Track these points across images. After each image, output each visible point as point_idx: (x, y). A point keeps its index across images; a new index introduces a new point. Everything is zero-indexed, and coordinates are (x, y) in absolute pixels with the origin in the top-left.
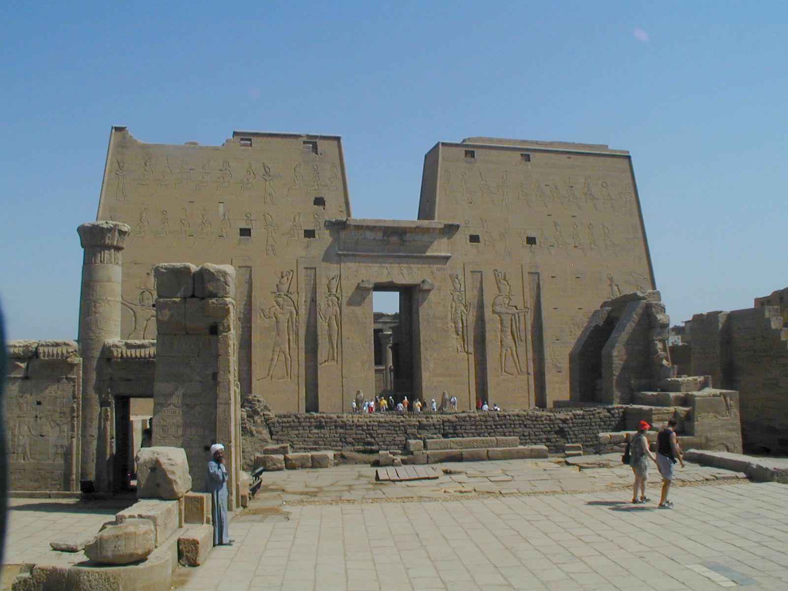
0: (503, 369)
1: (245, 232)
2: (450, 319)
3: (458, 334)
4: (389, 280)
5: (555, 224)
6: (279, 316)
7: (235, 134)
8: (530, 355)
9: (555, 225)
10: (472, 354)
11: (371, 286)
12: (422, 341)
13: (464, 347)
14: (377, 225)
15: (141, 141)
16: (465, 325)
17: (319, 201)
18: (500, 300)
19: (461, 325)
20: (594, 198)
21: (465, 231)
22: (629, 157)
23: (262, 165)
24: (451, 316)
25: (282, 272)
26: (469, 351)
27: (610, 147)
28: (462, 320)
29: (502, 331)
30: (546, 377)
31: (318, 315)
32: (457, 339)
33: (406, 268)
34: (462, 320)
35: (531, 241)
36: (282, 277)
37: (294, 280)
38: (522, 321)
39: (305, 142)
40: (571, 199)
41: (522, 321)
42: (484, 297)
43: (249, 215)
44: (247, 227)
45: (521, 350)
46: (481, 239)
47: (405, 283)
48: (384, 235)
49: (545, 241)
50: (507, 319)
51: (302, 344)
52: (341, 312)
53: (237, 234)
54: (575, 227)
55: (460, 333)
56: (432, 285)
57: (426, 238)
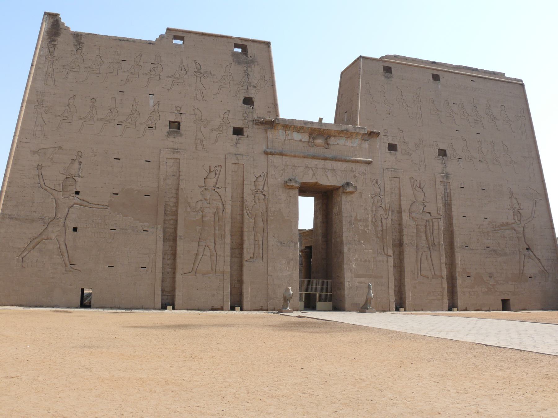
1: (175, 126)
2: (370, 221)
3: (378, 237)
4: (314, 180)
7: (168, 29)
8: (443, 259)
11: (297, 185)
12: (345, 242)
15: (74, 28)
16: (384, 228)
17: (248, 101)
19: (380, 228)
22: (523, 85)
23: (194, 62)
25: (210, 167)
27: (506, 76)
28: (382, 223)
30: (458, 281)
31: (245, 212)
34: (382, 223)
35: (443, 153)
37: (222, 176)
39: (236, 46)
40: (475, 118)
41: (435, 227)
42: (402, 203)
43: (179, 109)
44: (176, 120)
47: (328, 183)
48: (310, 137)
51: (228, 240)
52: (267, 208)
53: (166, 126)
55: (380, 235)
56: (356, 188)
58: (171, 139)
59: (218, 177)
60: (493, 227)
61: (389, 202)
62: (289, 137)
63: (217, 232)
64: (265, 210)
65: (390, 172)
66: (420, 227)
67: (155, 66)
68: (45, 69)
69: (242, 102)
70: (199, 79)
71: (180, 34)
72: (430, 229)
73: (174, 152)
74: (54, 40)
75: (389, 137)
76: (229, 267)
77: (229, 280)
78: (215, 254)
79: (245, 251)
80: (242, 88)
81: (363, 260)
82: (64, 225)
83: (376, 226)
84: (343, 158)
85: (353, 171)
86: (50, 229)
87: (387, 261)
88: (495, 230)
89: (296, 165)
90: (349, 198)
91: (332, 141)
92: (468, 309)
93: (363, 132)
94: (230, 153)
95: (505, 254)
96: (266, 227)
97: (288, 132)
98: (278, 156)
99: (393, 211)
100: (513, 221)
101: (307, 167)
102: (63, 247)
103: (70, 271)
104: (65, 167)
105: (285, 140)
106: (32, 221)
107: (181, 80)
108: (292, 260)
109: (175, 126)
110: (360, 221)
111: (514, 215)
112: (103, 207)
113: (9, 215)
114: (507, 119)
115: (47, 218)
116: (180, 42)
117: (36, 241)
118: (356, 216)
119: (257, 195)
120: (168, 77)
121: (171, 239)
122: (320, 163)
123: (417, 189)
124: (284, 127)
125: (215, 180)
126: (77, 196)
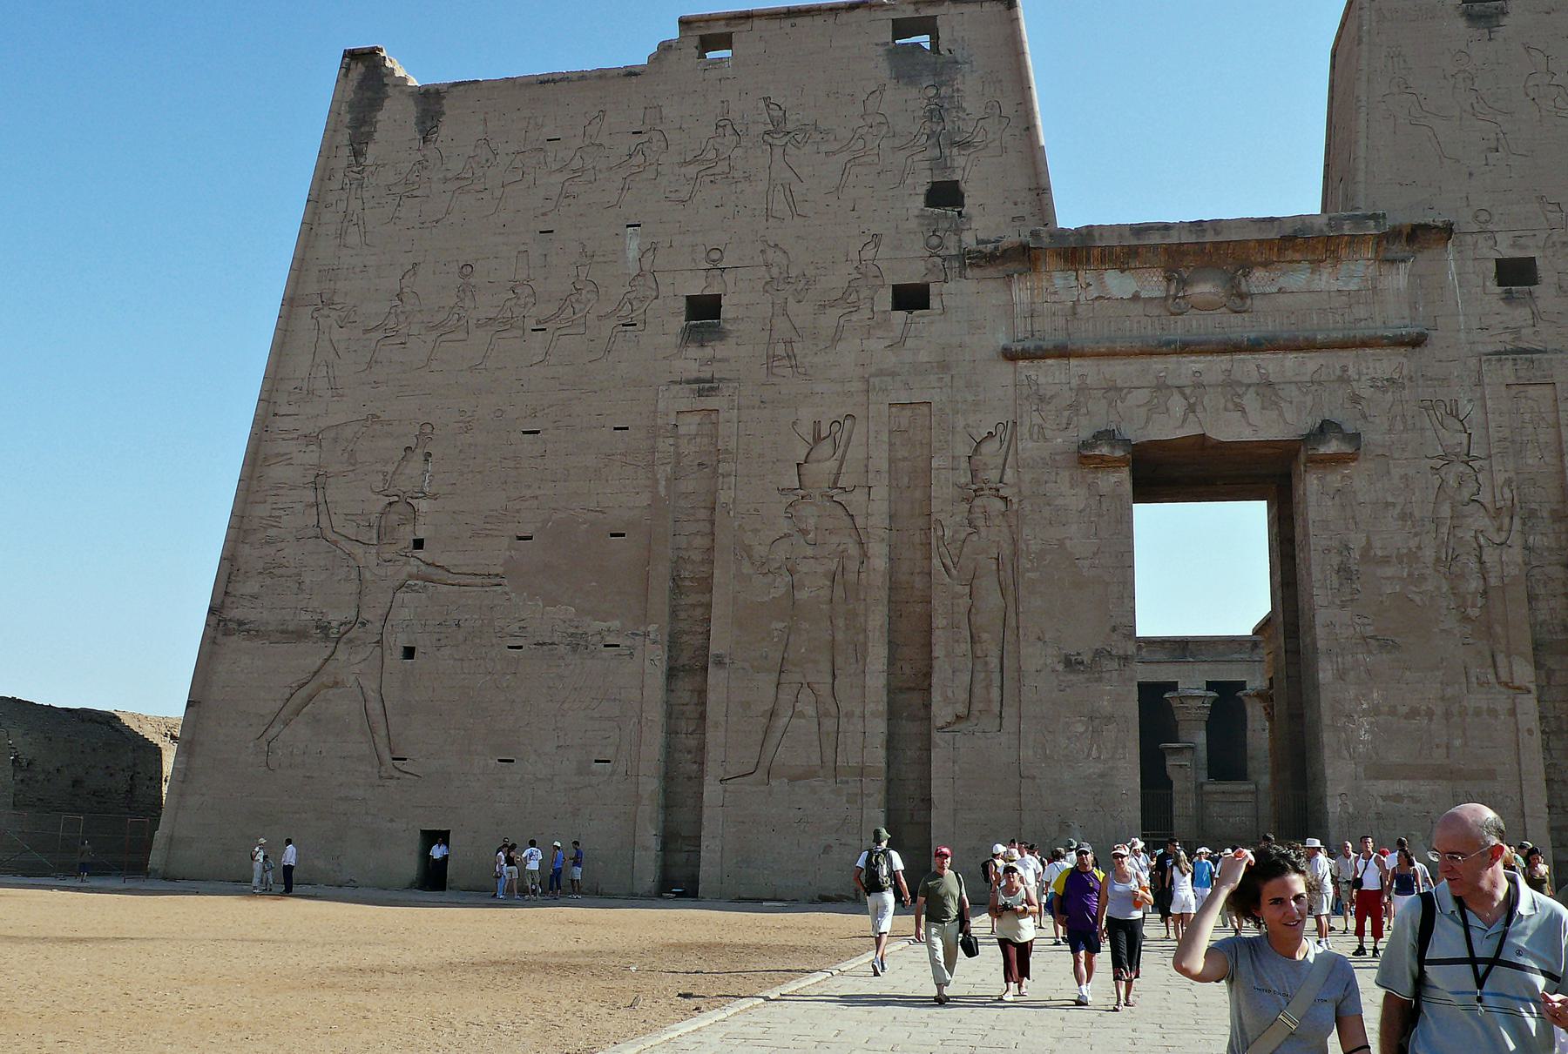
1: (704, 310)
3: (1466, 619)
4: (1191, 430)
6: (803, 568)
7: (685, 23)
11: (1119, 453)
12: (1321, 644)
13: (1495, 666)
14: (1136, 243)
16: (1493, 582)
17: (945, 195)
19: (1474, 584)
23: (762, 104)
25: (817, 423)
28: (1481, 562)
31: (936, 562)
33: (1252, 390)
34: (1481, 562)
36: (818, 439)
37: (855, 453)
43: (715, 255)
47: (1247, 435)
48: (1169, 280)
52: (1015, 542)
55: (1474, 612)
56: (1355, 438)
57: (1325, 280)
58: (693, 351)
59: (845, 452)
61: (1508, 482)
62: (1093, 292)
63: (840, 636)
64: (1007, 550)
67: (644, 138)
68: (342, 206)
69: (922, 198)
70: (778, 152)
71: (719, 28)
73: (700, 393)
74: (363, 122)
75: (1499, 237)
76: (882, 753)
77: (880, 797)
78: (833, 710)
79: (936, 697)
80: (920, 157)
81: (1404, 710)
82: (379, 643)
84: (1301, 335)
86: (341, 655)
87: (1513, 712)
89: (1119, 383)
90: (1334, 479)
91: (1259, 280)
93: (1371, 229)
94: (881, 373)
96: (1011, 609)
97: (1087, 276)
98: (1049, 361)
101: (1161, 387)
102: (375, 706)
103: (392, 778)
104: (385, 474)
105: (1075, 303)
106: (300, 635)
107: (722, 167)
108: (1110, 719)
109: (704, 310)
110: (1386, 561)
112: (486, 581)
113: (241, 623)
115: (334, 624)
116: (727, 53)
117: (304, 692)
118: (1369, 545)
119: (978, 502)
120: (686, 163)
121: (688, 666)
122: (1213, 367)
124: (1066, 260)
125: (832, 465)
126: (420, 554)
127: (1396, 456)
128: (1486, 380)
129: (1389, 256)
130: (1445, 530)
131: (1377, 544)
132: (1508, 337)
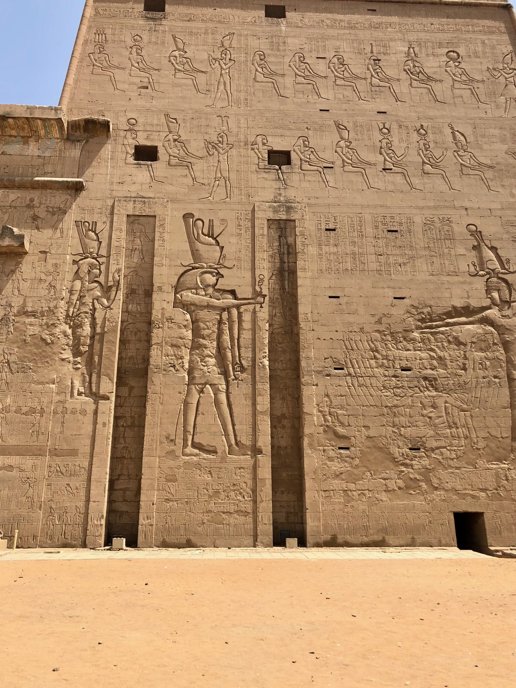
0: (190, 438)
3: (77, 353)
5: (338, 125)
8: (264, 402)
9: (338, 125)
10: (108, 399)
16: (98, 330)
18: (194, 277)
20: (429, 78)
21: (125, 137)
24: (67, 311)
26: (102, 392)
28: (94, 318)
29: (196, 346)
32: (75, 363)
35: (280, 158)
38: (247, 325)
40: (375, 81)
41: (247, 325)
45: (241, 391)
46: (161, 152)
49: (312, 157)
50: (209, 318)
54: (386, 131)
57: (32, 149)
60: (423, 320)
61: (119, 271)
65: (131, 205)
66: (202, 325)
72: (231, 329)
75: (139, 134)
81: (24, 410)
83: (76, 327)
85: (33, 207)
87: (96, 412)
88: (431, 327)
92: (340, 540)
95: (463, 387)
99: (131, 293)
100: (487, 302)
110: (33, 314)
111: (488, 291)
114: (464, 78)
123: (202, 237)
127: (53, 252)
128: (116, 211)
129: (72, 138)
130: (75, 297)
131: (30, 304)
132: (133, 188)
